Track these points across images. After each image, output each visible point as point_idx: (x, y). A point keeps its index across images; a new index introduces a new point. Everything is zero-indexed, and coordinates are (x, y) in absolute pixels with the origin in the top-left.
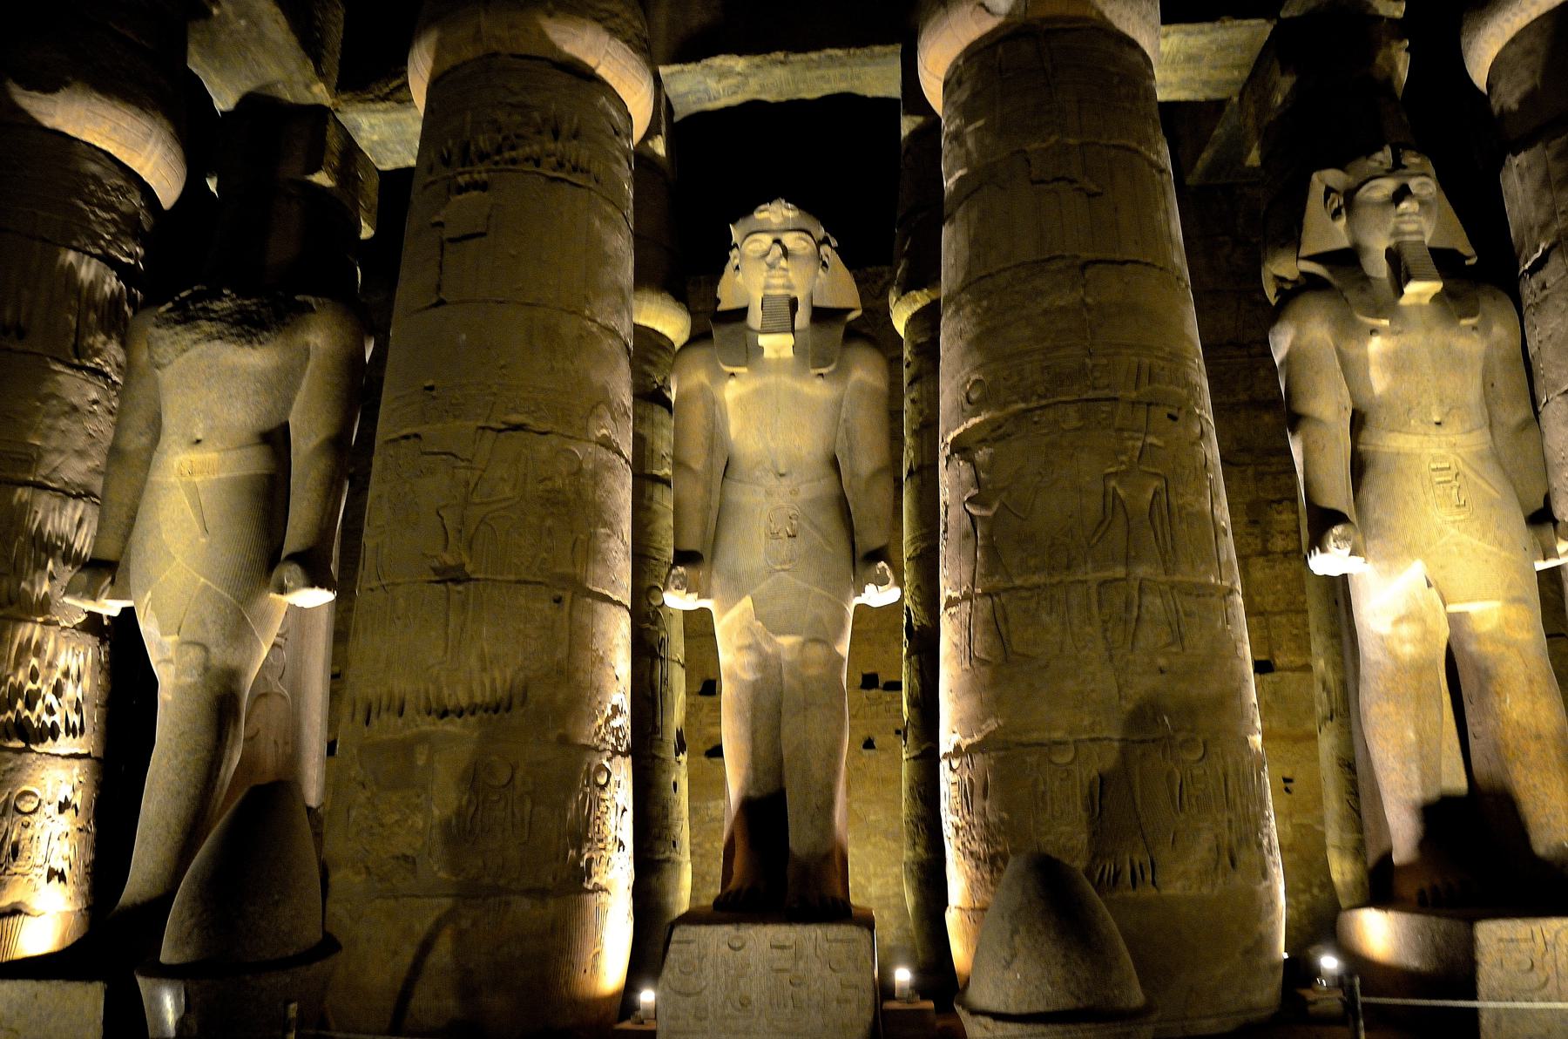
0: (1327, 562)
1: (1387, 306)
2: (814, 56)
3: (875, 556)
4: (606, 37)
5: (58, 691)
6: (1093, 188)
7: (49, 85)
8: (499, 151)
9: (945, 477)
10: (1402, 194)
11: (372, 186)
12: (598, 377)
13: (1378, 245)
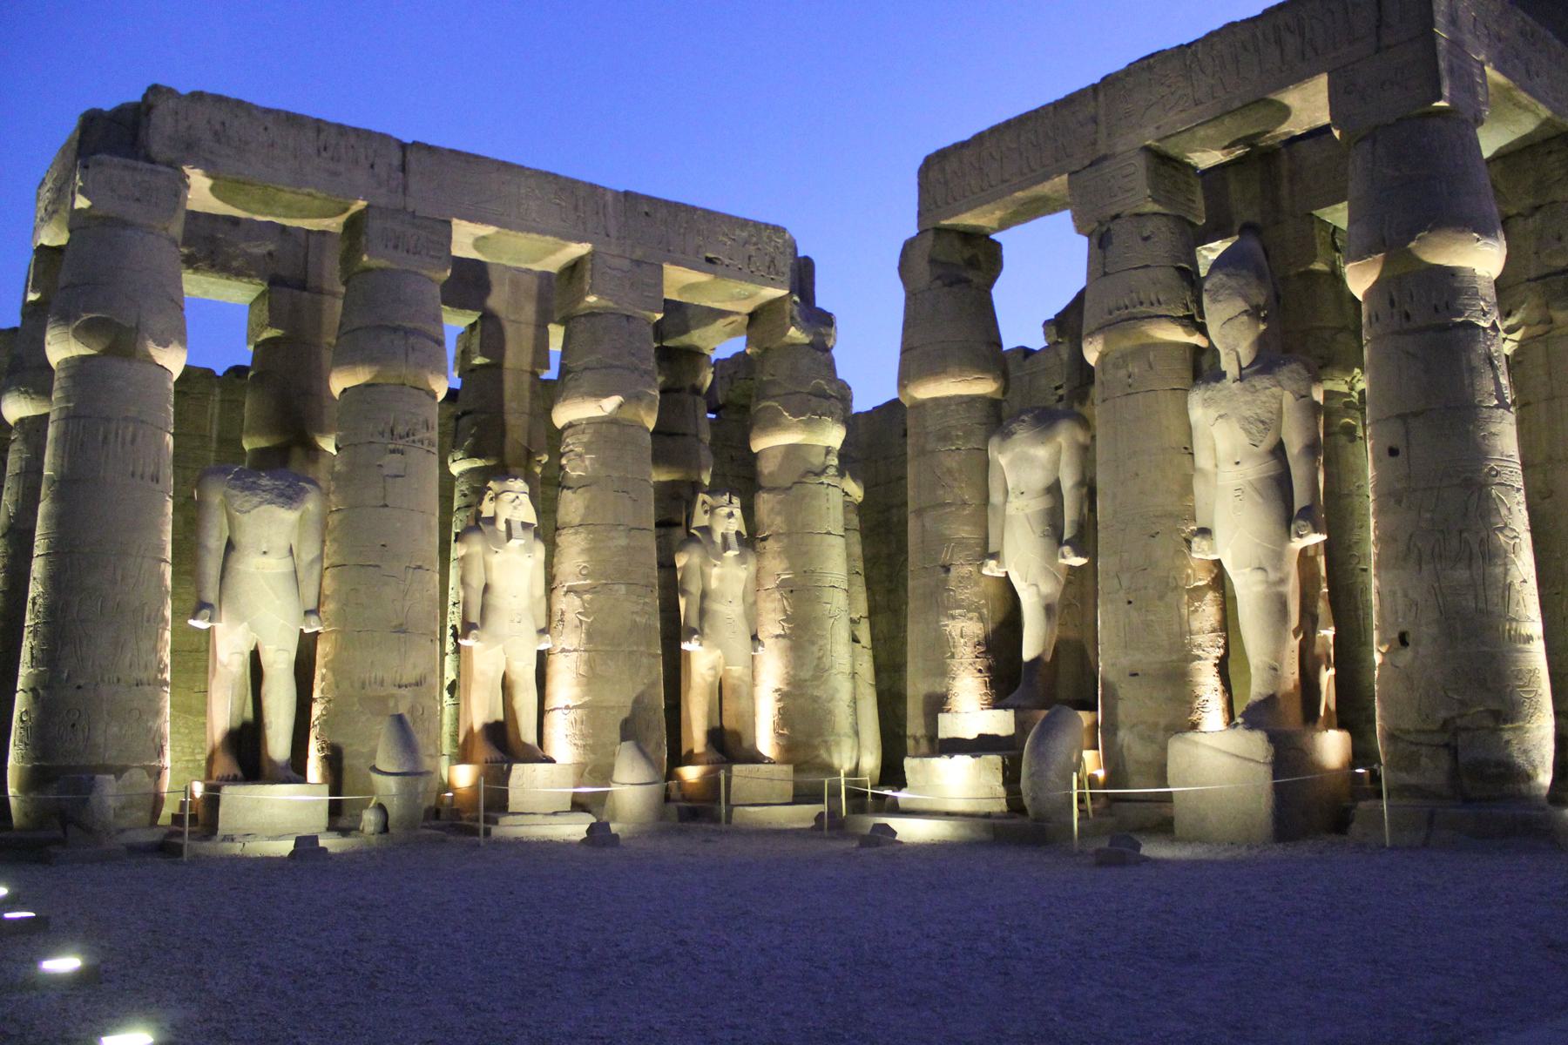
1: (719, 557)
10: (731, 515)
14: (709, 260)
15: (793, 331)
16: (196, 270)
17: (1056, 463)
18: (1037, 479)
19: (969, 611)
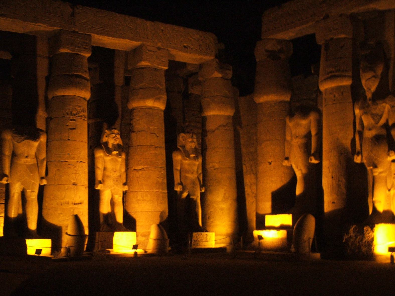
6: (158, 135)
10: (193, 141)
14: (185, 47)
17: (309, 126)
18: (302, 131)
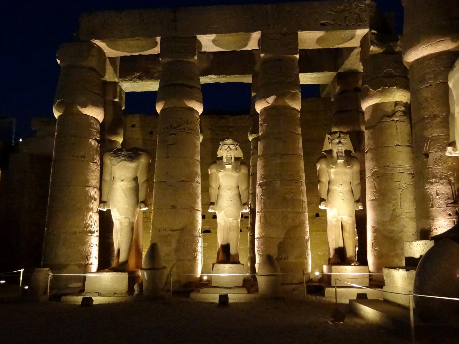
0: (322, 207)
1: (335, 163)
2: (232, 76)
3: (245, 204)
4: (196, 102)
5: (95, 224)
7: (85, 106)
8: (177, 127)
9: (257, 190)
11: (124, 96)
12: (196, 170)
13: (335, 151)
14: (323, 25)
15: (372, 48)
16: (142, 80)
19: (441, 179)
